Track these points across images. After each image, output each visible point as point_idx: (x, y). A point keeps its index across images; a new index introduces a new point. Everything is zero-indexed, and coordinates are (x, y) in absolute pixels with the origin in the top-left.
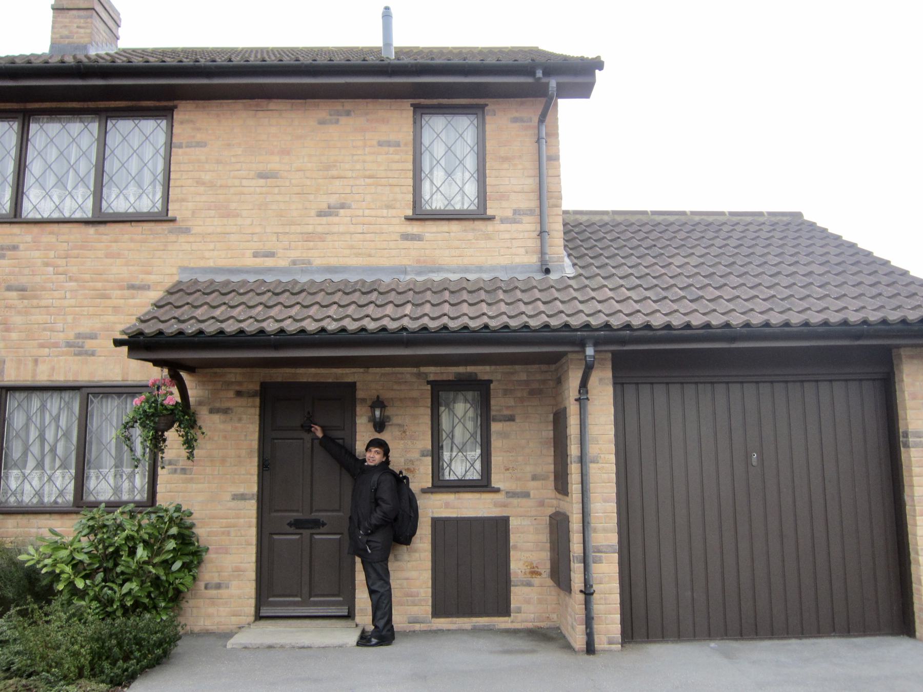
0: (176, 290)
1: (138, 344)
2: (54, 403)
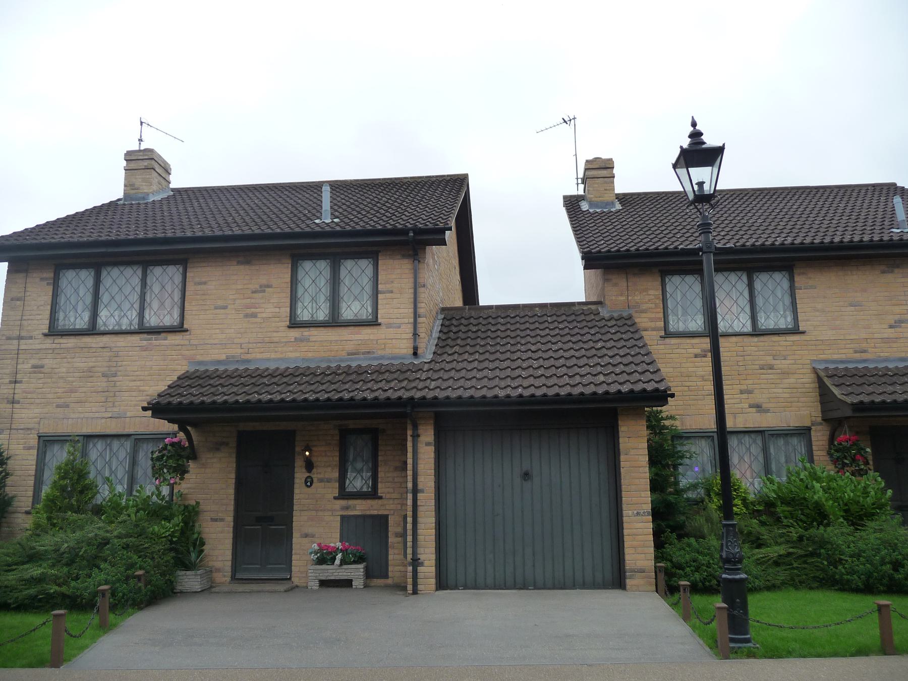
1: (158, 409)
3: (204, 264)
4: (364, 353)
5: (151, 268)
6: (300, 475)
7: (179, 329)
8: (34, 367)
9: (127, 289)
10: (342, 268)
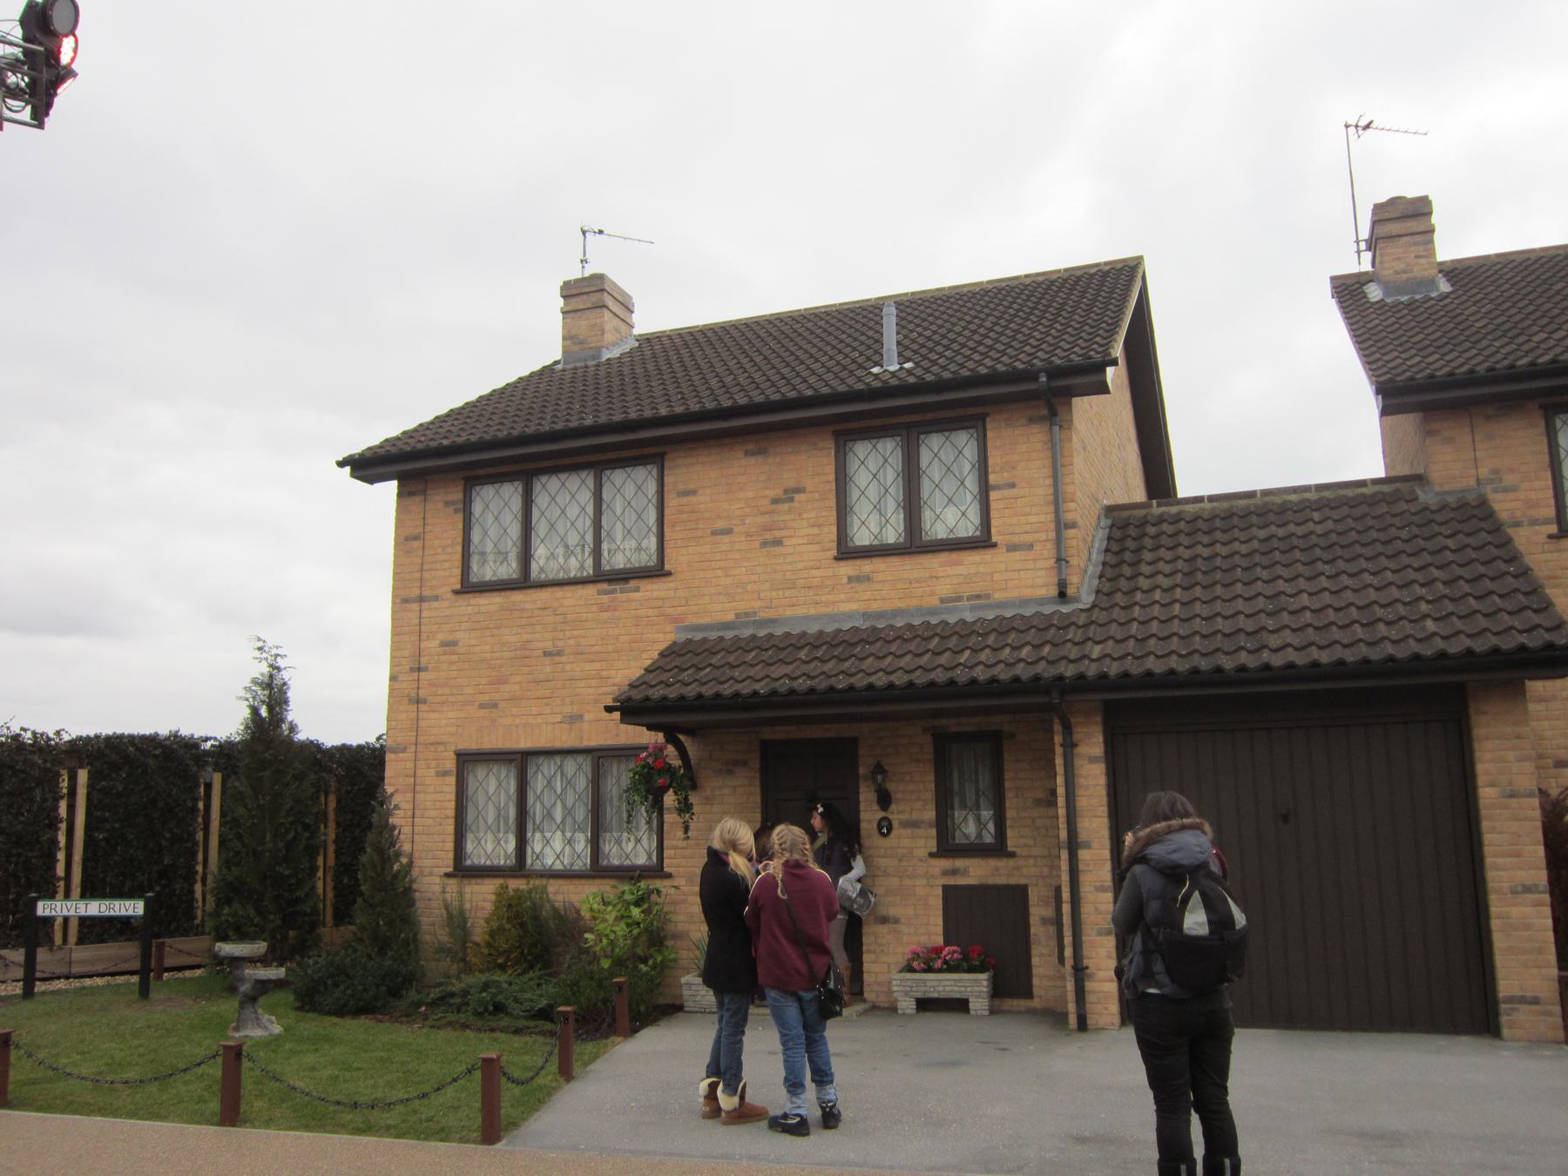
0: (670, 652)
1: (630, 709)
2: (570, 765)
3: (690, 460)
4: (970, 598)
5: (608, 472)
7: (658, 571)
8: (444, 644)
9: (573, 511)
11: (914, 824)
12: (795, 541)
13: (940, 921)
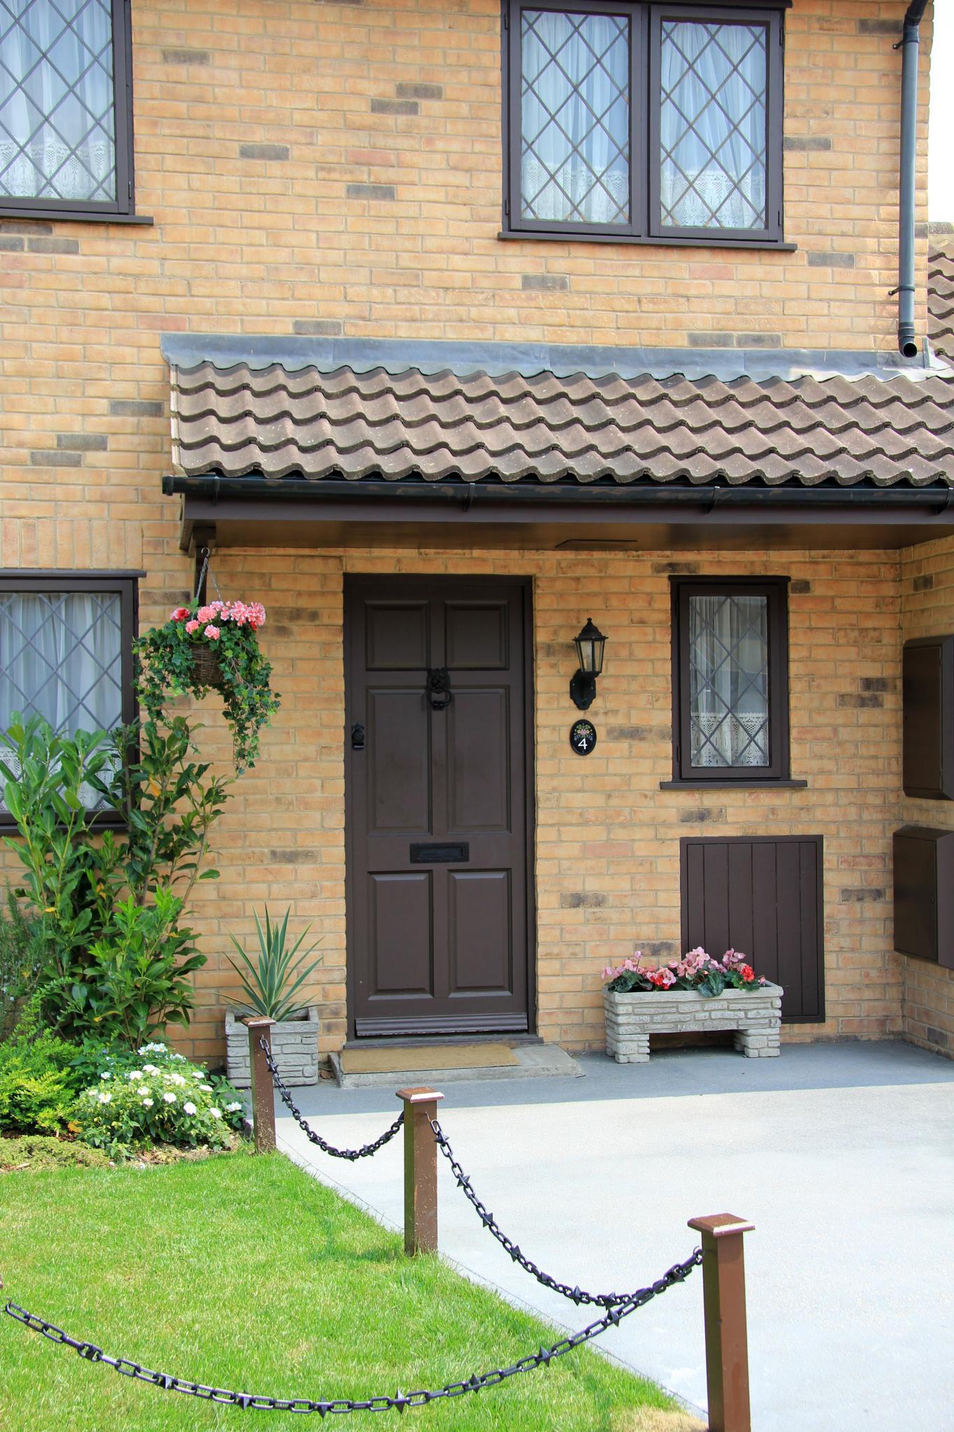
4: (742, 341)
6: (554, 713)
7: (117, 214)
10: (668, 50)
11: (634, 734)
12: (419, 193)
13: (676, 899)
